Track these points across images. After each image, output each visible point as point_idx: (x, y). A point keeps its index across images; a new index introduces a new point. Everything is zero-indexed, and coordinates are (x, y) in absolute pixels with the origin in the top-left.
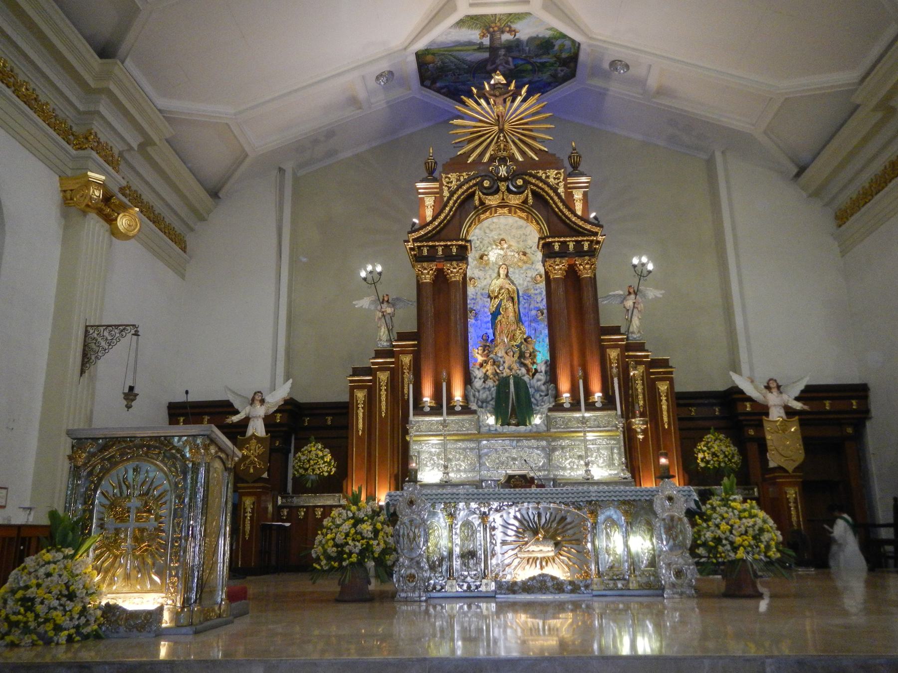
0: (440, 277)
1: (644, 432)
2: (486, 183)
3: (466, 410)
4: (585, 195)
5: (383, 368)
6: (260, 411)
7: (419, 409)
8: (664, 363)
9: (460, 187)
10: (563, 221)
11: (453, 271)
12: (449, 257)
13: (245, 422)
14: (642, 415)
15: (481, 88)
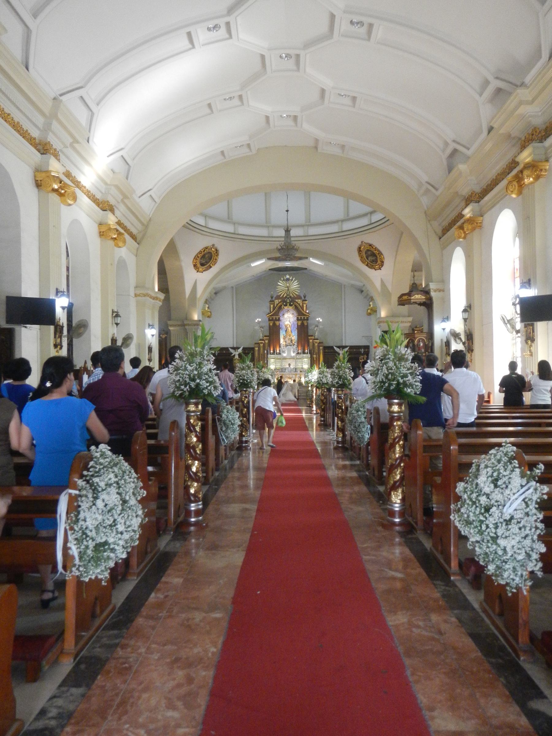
0: (274, 324)
1: (316, 358)
2: (284, 304)
3: (280, 354)
4: (306, 306)
5: (262, 343)
6: (237, 353)
7: (270, 354)
8: (322, 343)
9: (279, 303)
10: (301, 312)
11: (277, 323)
12: (276, 320)
13: (234, 355)
14: (316, 354)
15: (284, 278)
